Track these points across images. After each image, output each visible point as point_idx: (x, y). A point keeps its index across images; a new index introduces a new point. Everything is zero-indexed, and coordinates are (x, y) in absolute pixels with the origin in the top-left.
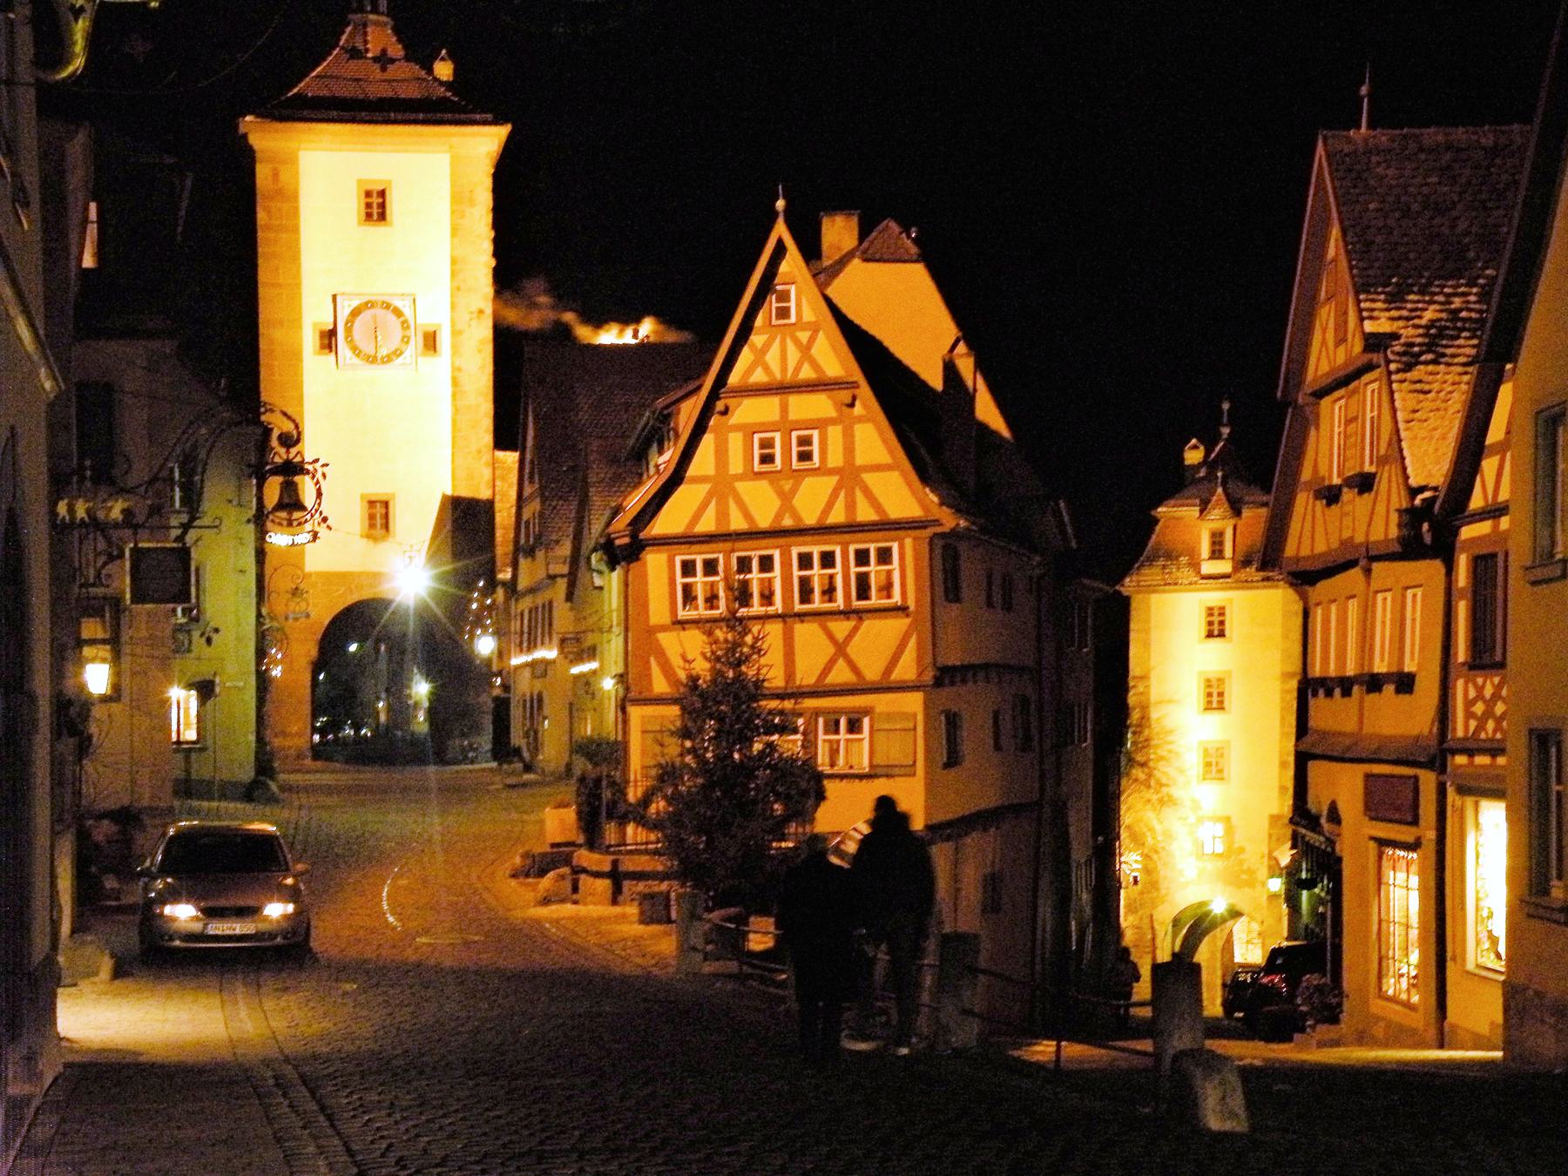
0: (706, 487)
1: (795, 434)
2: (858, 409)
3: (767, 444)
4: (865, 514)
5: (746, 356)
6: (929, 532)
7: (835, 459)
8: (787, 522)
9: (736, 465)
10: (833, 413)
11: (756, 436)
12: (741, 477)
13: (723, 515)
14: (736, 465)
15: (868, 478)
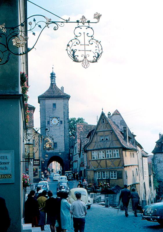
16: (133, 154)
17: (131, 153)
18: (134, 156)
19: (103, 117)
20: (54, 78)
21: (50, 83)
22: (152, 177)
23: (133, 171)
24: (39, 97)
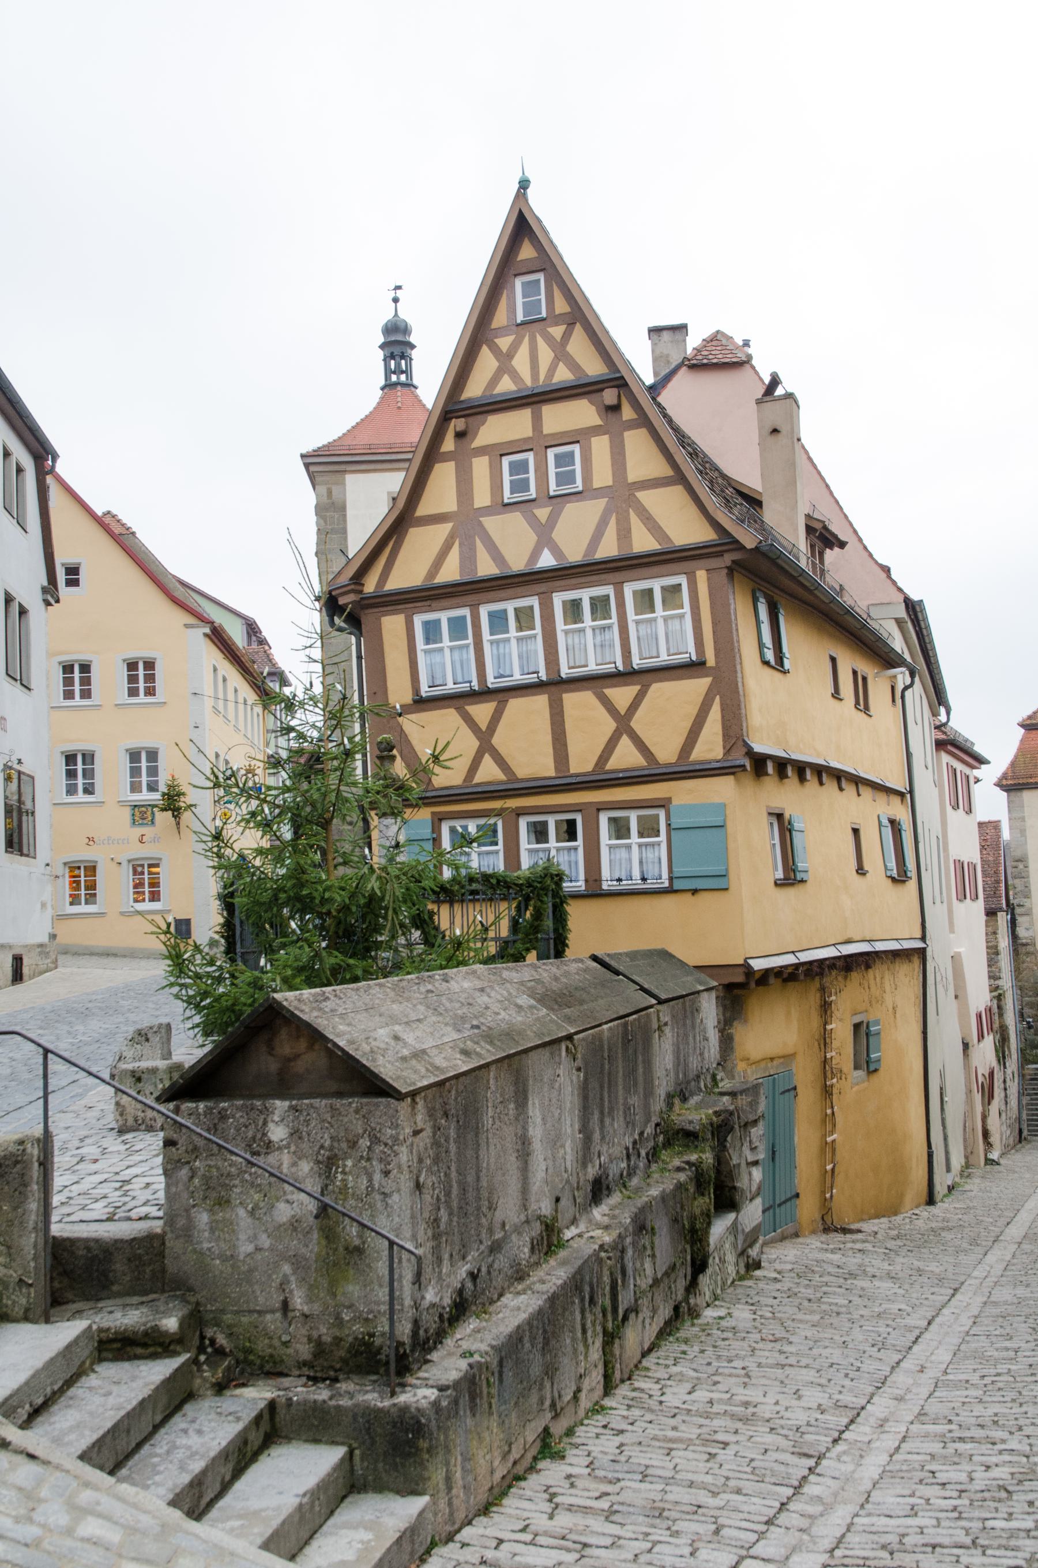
0: (446, 528)
1: (551, 453)
2: (628, 413)
3: (519, 468)
4: (643, 542)
5: (486, 363)
6: (728, 559)
7: (603, 476)
8: (547, 560)
9: (482, 498)
10: (600, 422)
11: (506, 461)
12: (487, 511)
13: (468, 559)
14: (482, 498)
15: (642, 495)
16: (861, 684)
17: (833, 660)
18: (863, 704)
19: (527, 252)
20: (397, 350)
21: (382, 382)
22: (1003, 918)
23: (856, 831)
24: (303, 456)
